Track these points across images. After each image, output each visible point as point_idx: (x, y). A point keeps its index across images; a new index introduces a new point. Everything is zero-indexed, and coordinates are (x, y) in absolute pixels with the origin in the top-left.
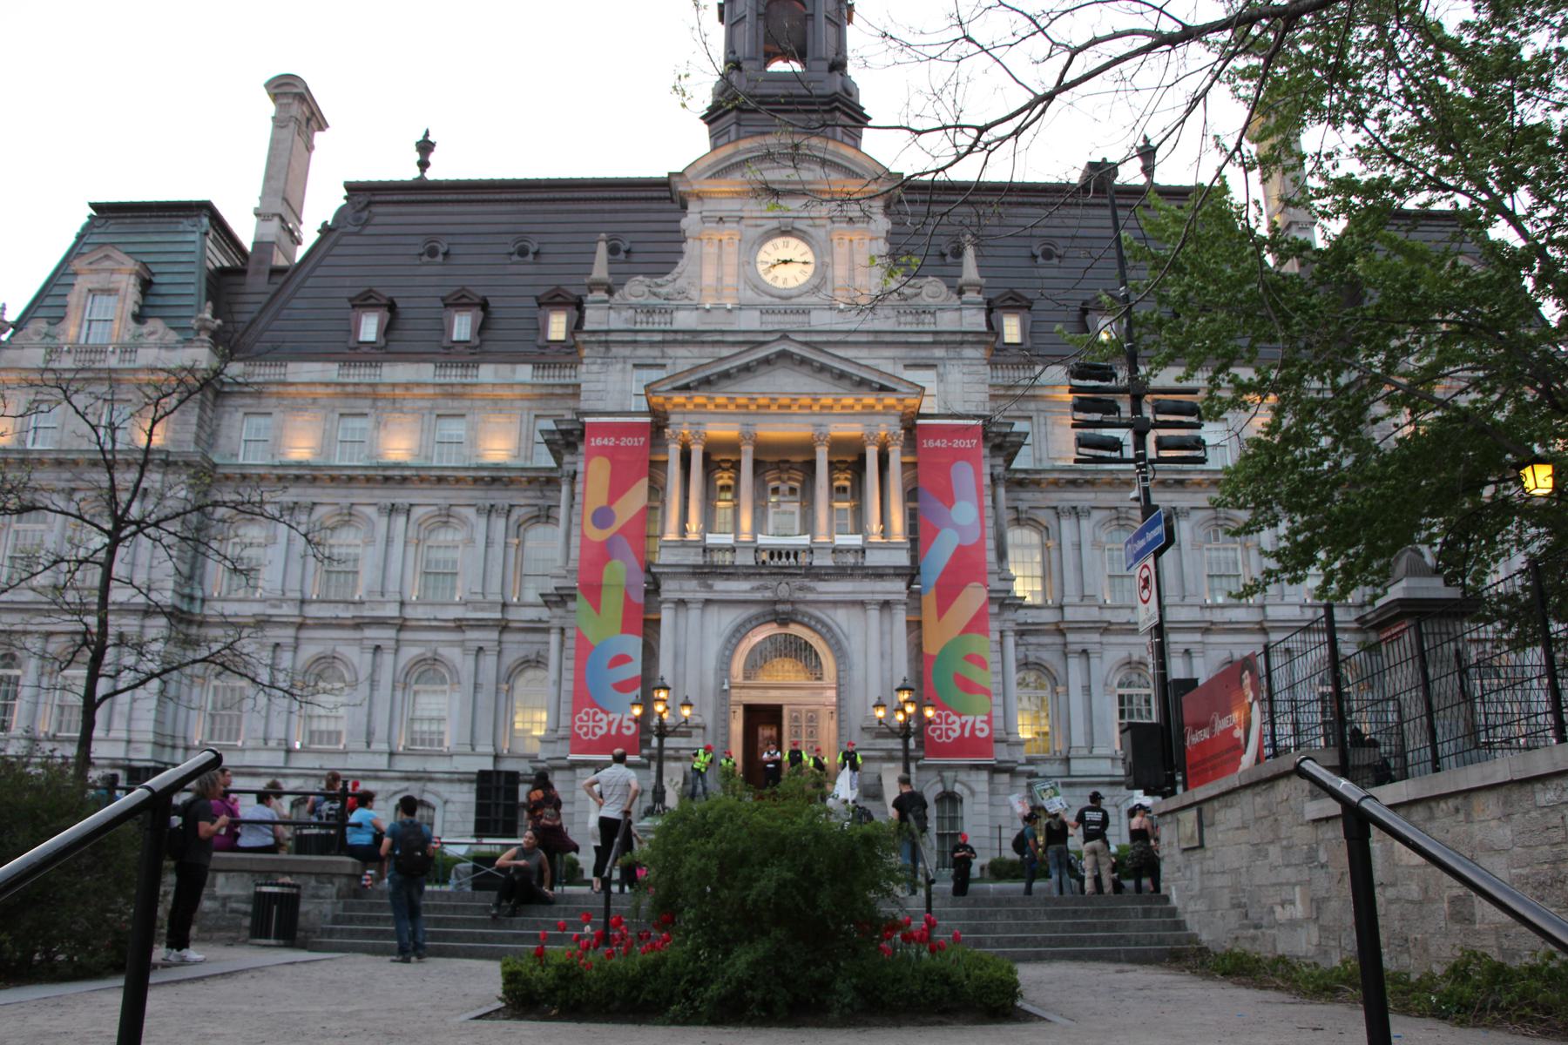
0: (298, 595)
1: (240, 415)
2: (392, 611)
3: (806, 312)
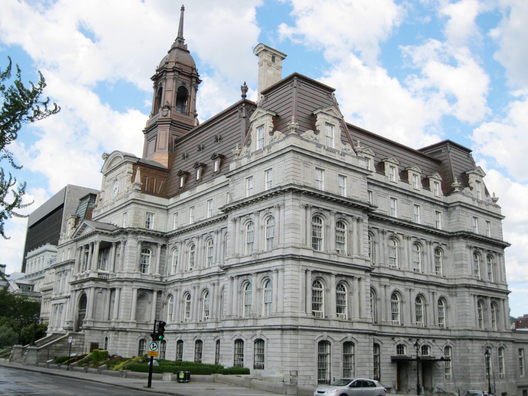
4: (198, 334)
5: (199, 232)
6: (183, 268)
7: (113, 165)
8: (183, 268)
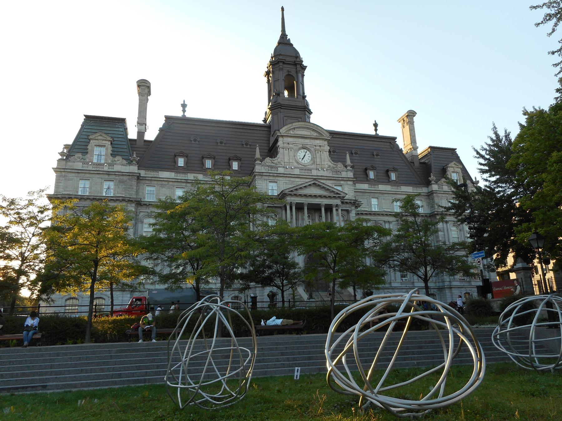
1: (145, 186)
3: (311, 170)
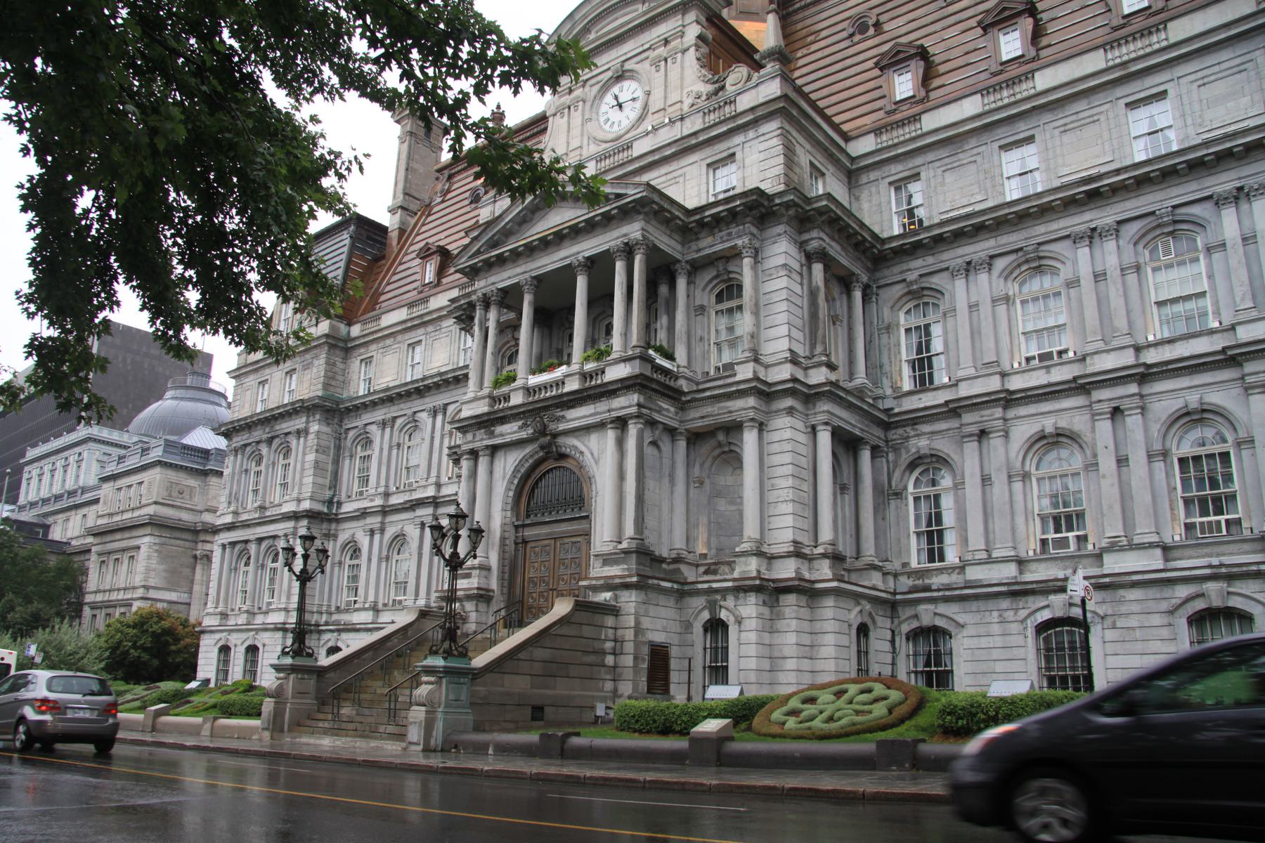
0: (381, 490)
2: (430, 492)
3: (629, 147)
4: (1212, 587)
5: (1104, 216)
6: (998, 354)
7: (592, 36)
8: (998, 354)
